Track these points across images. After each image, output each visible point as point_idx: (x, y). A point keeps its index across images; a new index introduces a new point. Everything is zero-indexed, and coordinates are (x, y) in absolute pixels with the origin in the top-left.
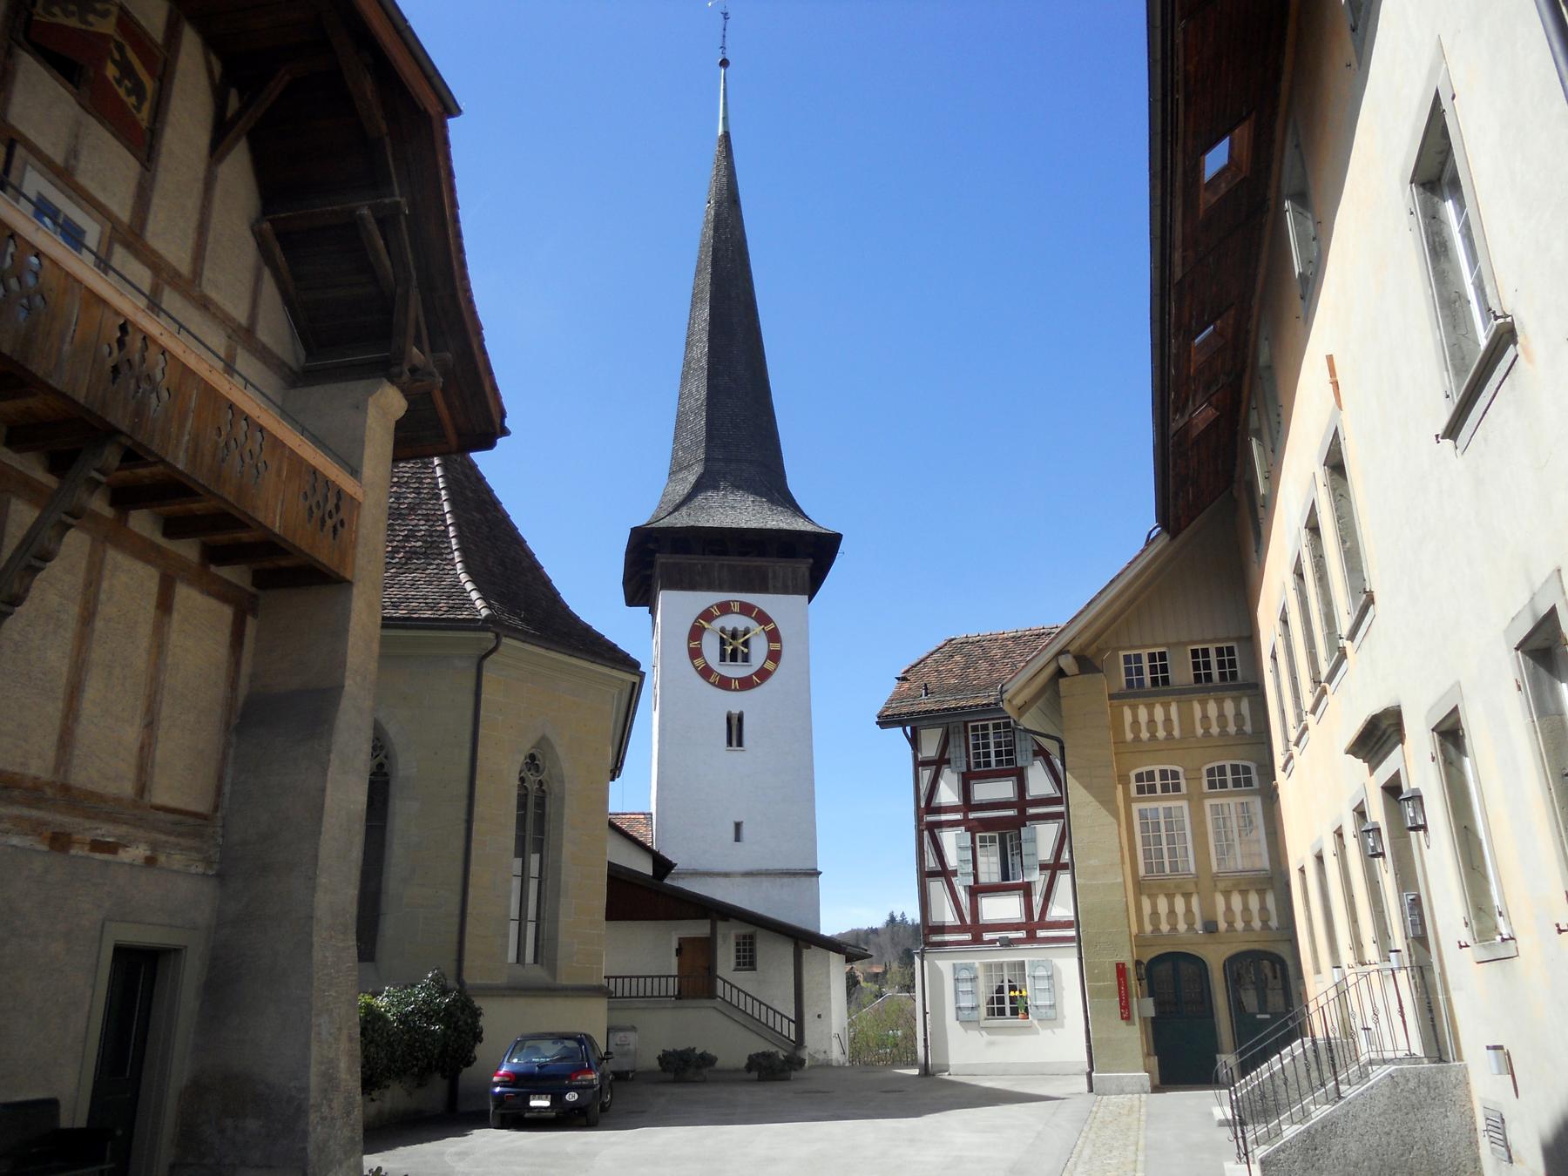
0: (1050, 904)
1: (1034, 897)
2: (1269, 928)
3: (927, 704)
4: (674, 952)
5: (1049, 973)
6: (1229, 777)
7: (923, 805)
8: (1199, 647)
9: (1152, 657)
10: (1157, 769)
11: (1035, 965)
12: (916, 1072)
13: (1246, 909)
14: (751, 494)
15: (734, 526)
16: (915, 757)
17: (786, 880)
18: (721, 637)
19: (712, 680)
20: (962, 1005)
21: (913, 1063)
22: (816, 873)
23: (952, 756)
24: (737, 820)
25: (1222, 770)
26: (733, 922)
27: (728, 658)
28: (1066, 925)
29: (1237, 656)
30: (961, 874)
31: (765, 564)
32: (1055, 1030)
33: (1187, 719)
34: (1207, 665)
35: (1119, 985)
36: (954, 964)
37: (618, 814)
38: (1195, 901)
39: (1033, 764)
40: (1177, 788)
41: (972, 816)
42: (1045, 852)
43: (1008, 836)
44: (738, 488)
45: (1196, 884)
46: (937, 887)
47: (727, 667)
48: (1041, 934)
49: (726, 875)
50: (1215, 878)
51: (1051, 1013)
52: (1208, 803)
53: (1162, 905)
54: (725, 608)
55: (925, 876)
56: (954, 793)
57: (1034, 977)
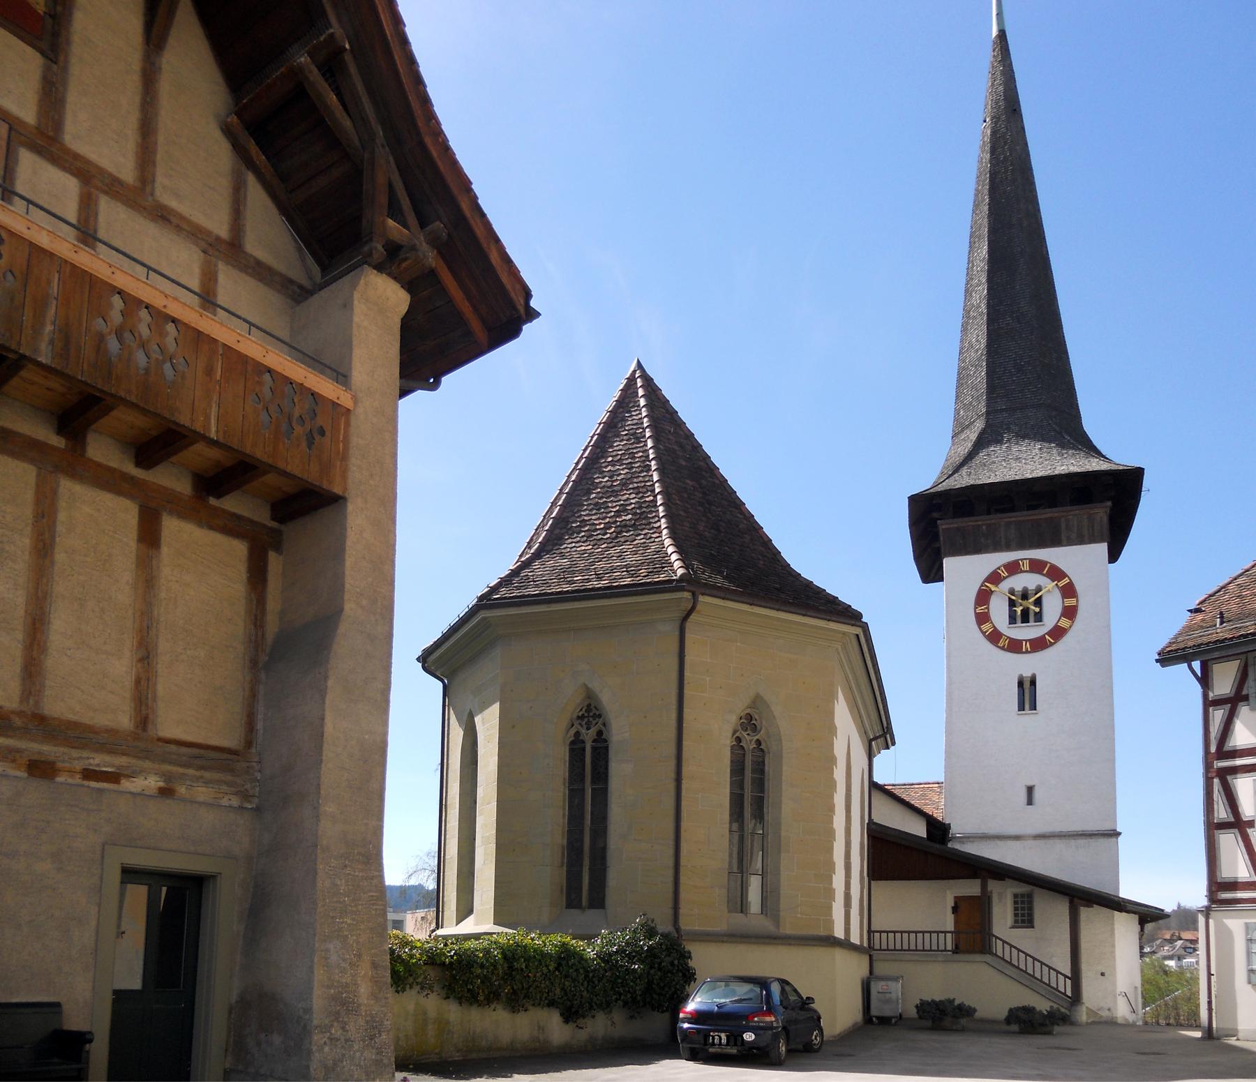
4: (949, 910)
7: (1213, 749)
12: (1198, 1034)
14: (1039, 441)
15: (1017, 478)
16: (1205, 696)
17: (1082, 842)
18: (1009, 598)
19: (1001, 644)
21: (1197, 1027)
22: (1117, 834)
24: (1030, 784)
26: (1009, 882)
27: (1019, 619)
31: (1056, 514)
36: (1246, 924)
37: (913, 784)
44: (1024, 437)
46: (1229, 842)
47: (1017, 629)
49: (1017, 838)
54: (1013, 568)
55: (1213, 828)
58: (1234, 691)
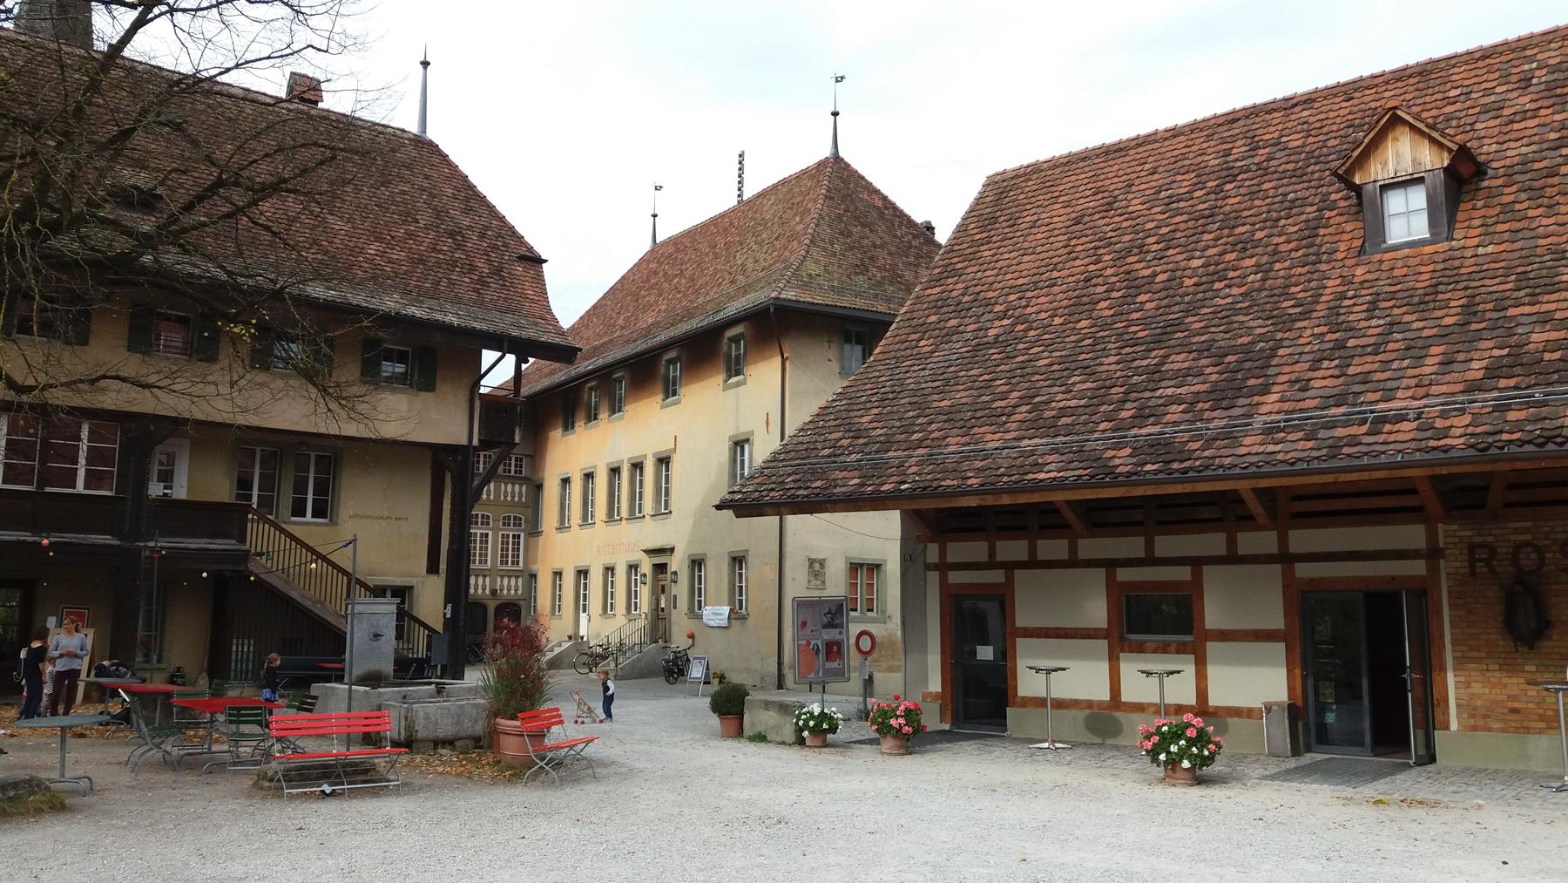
6: (512, 522)
40: (488, 524)
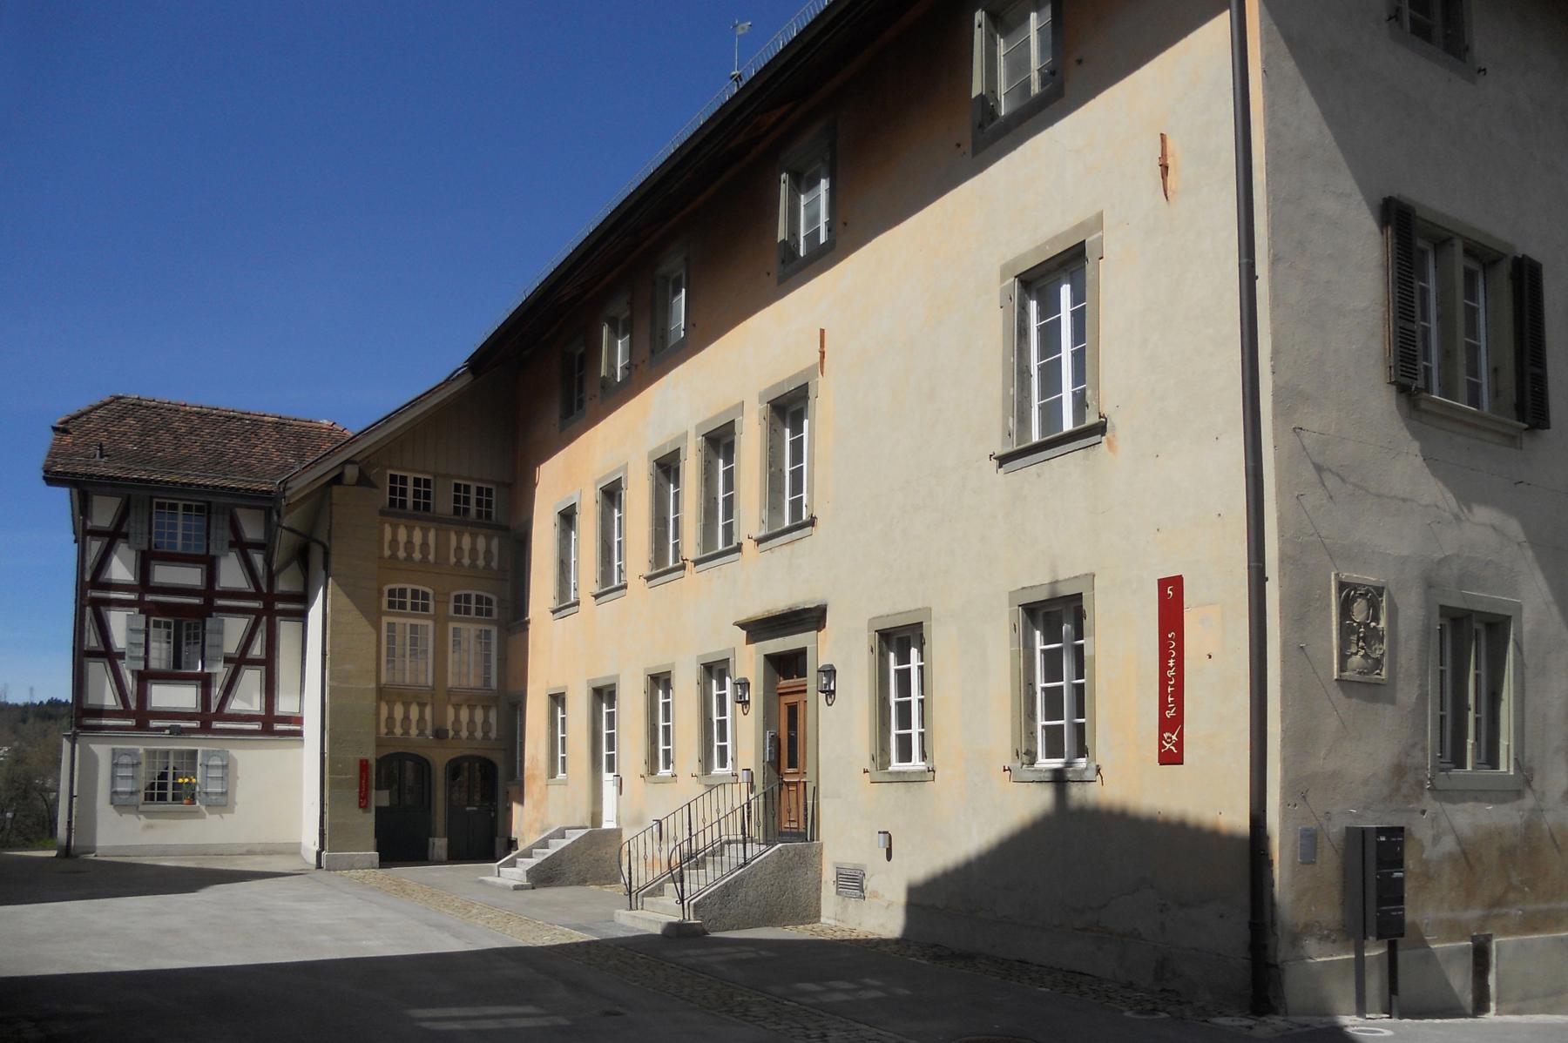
0: (230, 698)
1: (213, 689)
2: (489, 739)
3: (103, 468)
5: (225, 763)
6: (473, 606)
7: (88, 578)
8: (484, 486)
9: (417, 482)
10: (409, 587)
11: (207, 754)
13: (471, 721)
20: (119, 789)
23: (132, 531)
25: (467, 598)
28: (249, 718)
29: (494, 499)
30: (131, 657)
32: (224, 815)
33: (442, 545)
34: (467, 500)
35: (361, 778)
36: (113, 750)
38: (428, 710)
39: (227, 555)
40: (425, 608)
41: (149, 598)
42: (231, 645)
43: (184, 624)
45: (432, 697)
46: (97, 671)
48: (217, 725)
50: (449, 692)
51: (222, 800)
52: (451, 625)
53: (399, 711)
56: (128, 569)
57: (207, 766)
58: (113, 526)
